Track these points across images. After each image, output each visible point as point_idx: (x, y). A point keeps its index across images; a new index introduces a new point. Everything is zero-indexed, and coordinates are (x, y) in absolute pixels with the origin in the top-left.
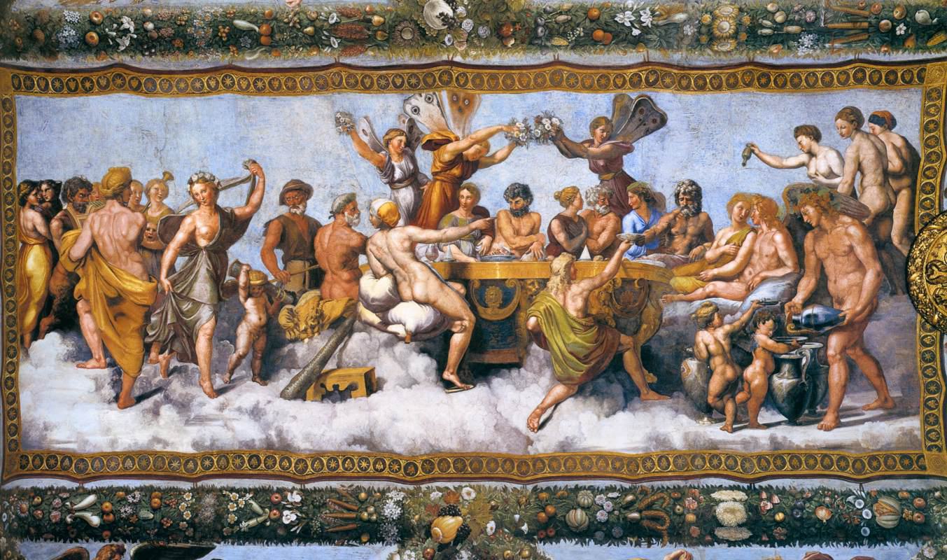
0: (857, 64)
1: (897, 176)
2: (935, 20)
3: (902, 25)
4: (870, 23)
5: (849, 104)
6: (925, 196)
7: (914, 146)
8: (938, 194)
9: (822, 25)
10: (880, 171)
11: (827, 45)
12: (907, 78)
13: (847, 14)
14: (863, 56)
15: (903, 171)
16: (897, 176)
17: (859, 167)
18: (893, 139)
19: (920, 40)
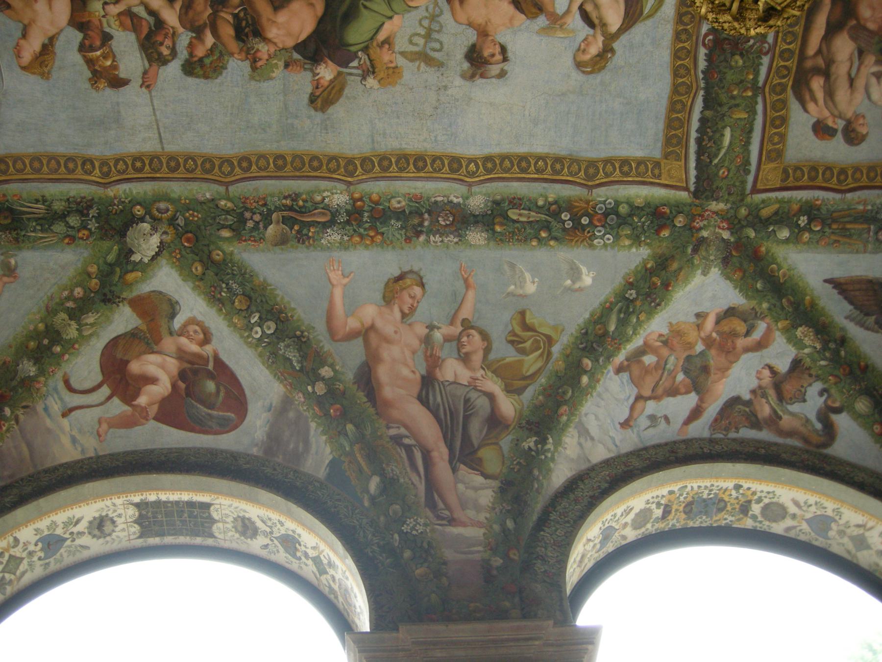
0: (844, 188)
1: (817, 71)
2: (771, 229)
3: (802, 225)
4: (830, 228)
5: (854, 148)
6: (791, 46)
7: (797, 103)
8: (778, 48)
9: (872, 227)
10: (833, 78)
11: (869, 207)
12: (799, 173)
13: (850, 236)
14: (838, 196)
15: (810, 75)
16: (817, 71)
17: (851, 81)
18: (817, 110)
19: (786, 210)
